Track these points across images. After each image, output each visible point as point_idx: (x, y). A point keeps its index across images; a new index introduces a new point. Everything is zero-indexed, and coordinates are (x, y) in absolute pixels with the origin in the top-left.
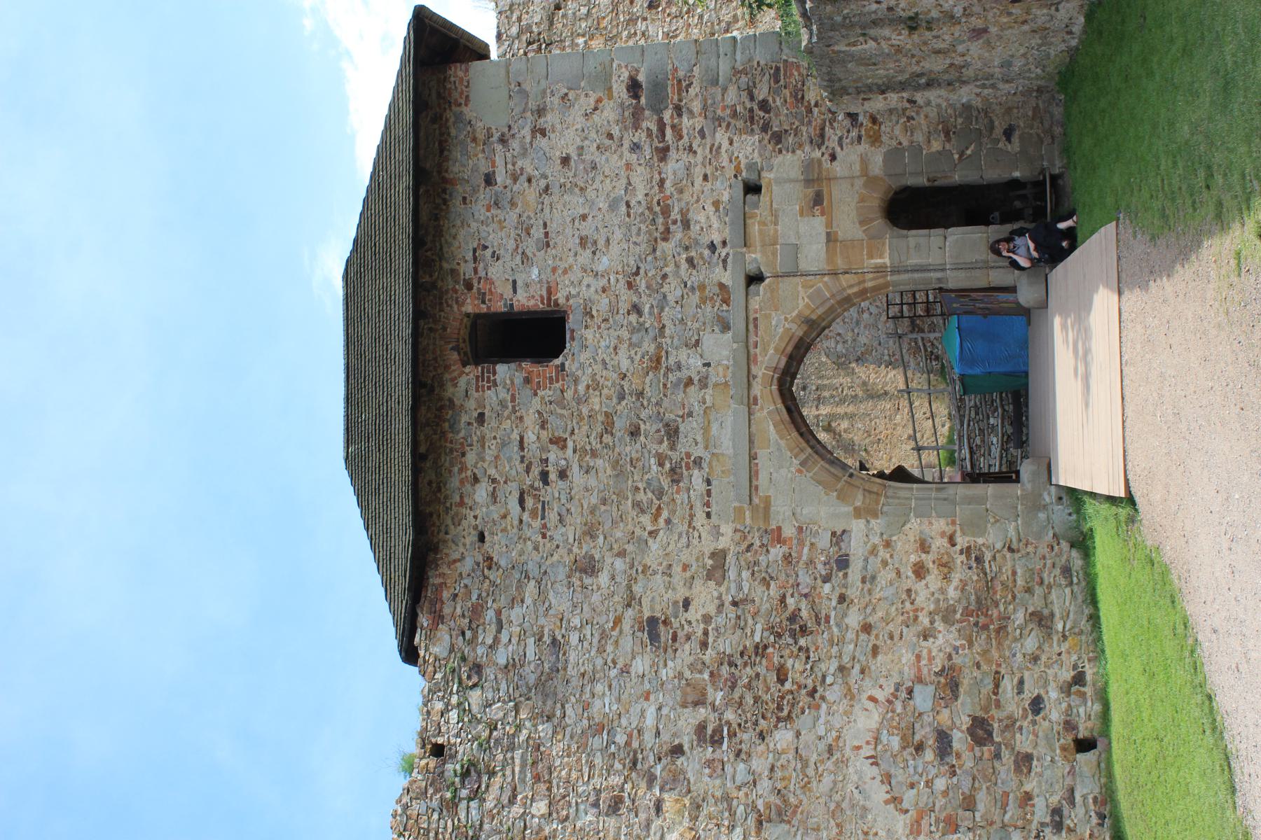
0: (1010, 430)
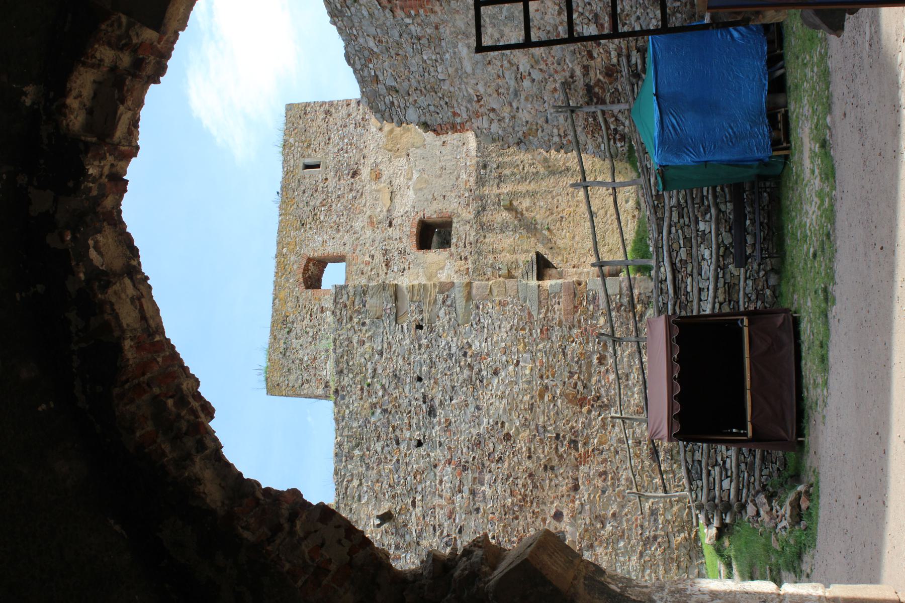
0: (728, 239)
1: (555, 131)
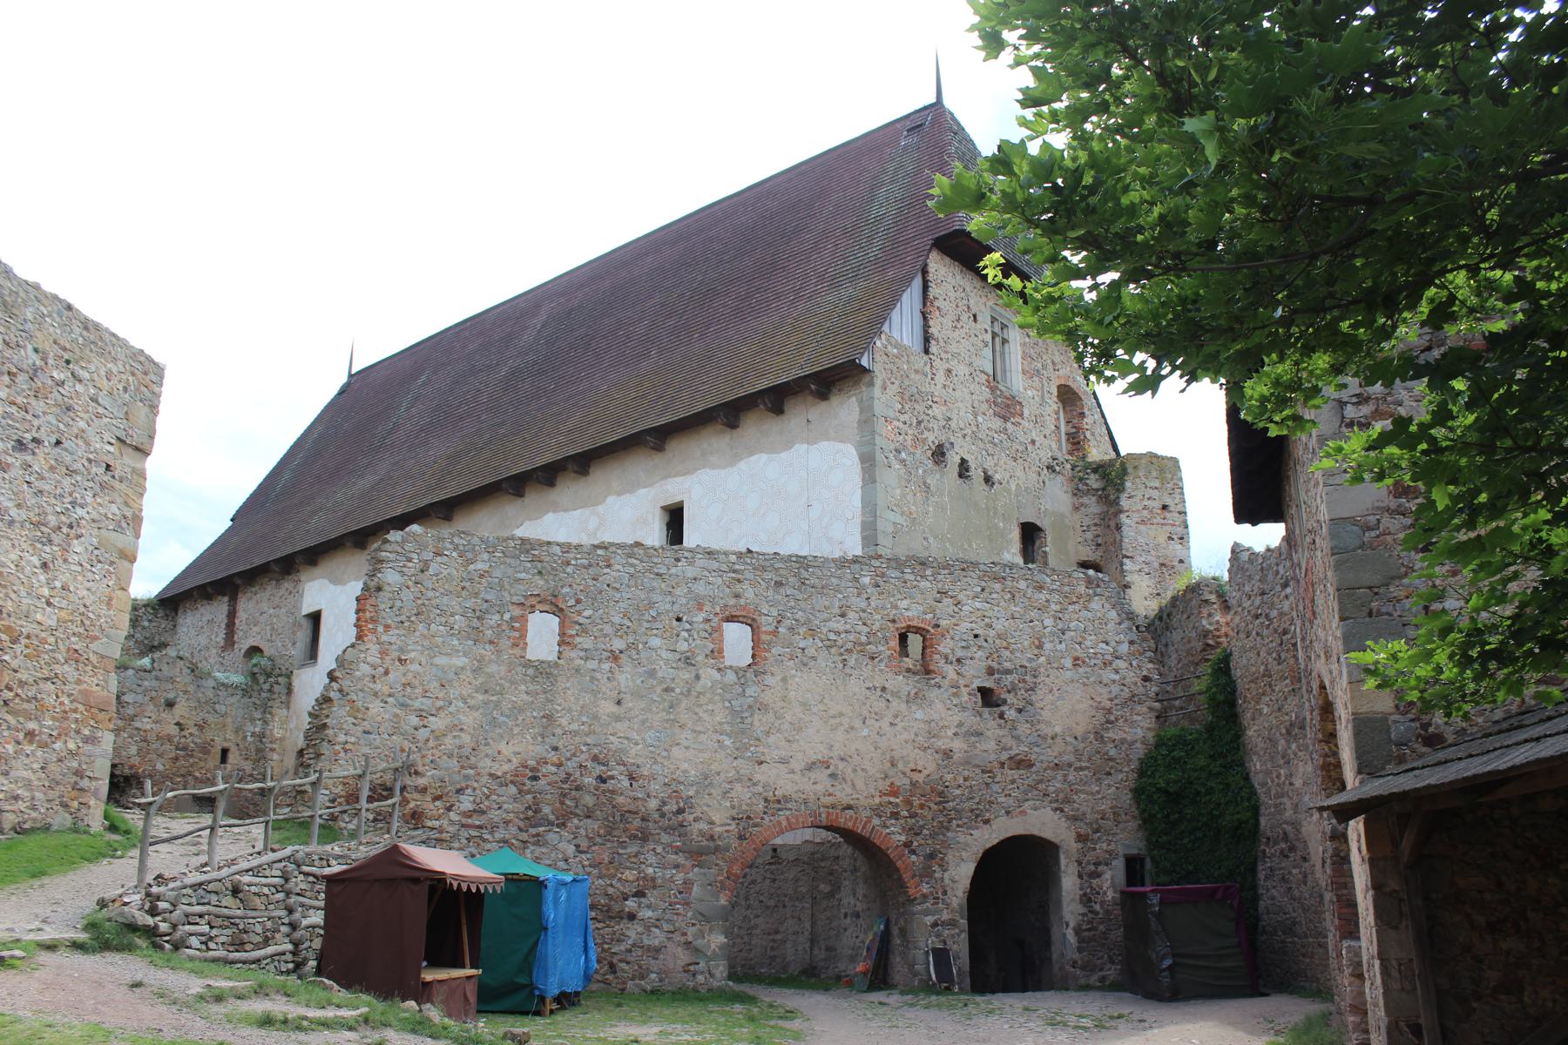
1: (353, 740)
